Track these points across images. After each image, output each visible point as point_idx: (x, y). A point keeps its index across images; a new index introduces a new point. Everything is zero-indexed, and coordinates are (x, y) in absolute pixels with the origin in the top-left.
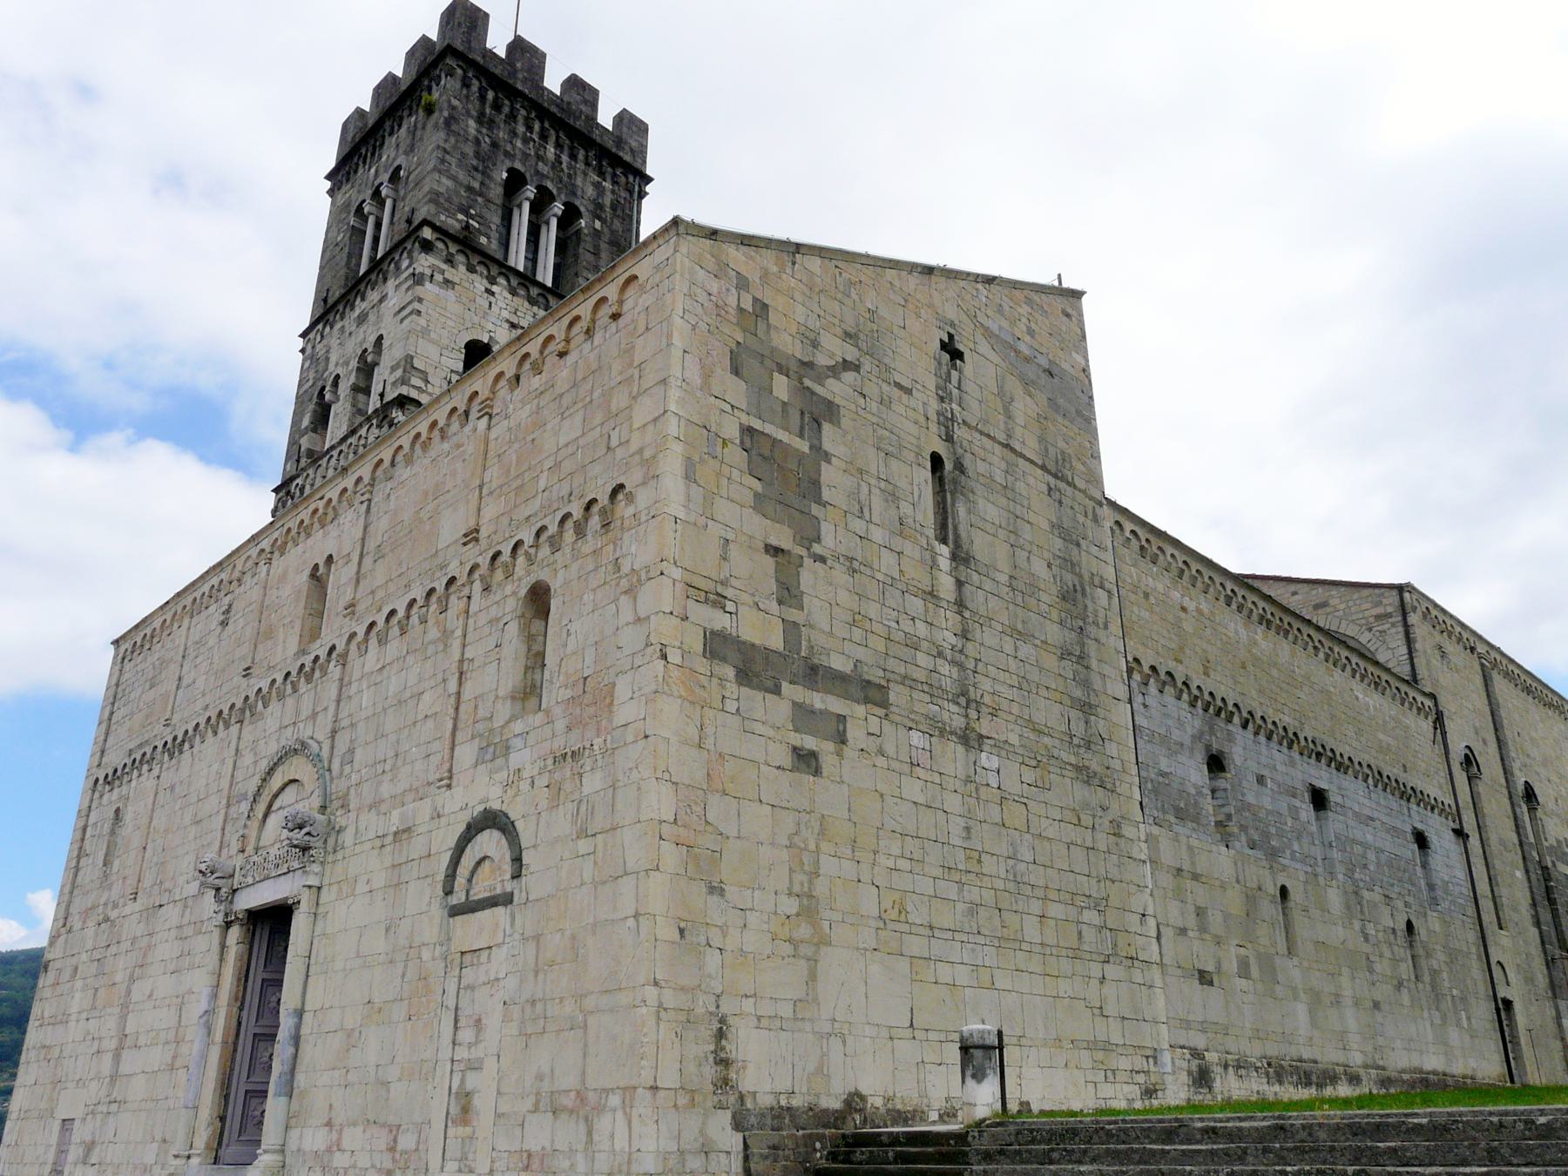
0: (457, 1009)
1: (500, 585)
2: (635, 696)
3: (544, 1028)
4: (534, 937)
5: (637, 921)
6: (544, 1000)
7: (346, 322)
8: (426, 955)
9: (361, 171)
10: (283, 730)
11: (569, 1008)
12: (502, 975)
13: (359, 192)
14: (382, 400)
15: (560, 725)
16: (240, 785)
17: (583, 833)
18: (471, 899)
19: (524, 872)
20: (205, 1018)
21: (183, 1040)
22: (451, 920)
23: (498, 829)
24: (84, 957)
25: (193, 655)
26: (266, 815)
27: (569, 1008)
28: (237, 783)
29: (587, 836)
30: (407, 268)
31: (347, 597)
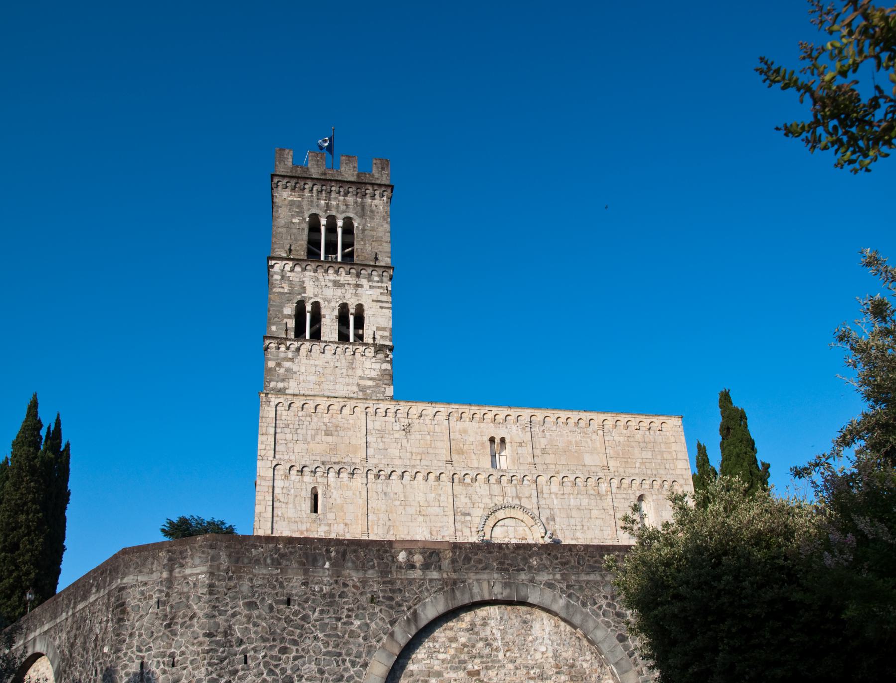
1: (625, 489)
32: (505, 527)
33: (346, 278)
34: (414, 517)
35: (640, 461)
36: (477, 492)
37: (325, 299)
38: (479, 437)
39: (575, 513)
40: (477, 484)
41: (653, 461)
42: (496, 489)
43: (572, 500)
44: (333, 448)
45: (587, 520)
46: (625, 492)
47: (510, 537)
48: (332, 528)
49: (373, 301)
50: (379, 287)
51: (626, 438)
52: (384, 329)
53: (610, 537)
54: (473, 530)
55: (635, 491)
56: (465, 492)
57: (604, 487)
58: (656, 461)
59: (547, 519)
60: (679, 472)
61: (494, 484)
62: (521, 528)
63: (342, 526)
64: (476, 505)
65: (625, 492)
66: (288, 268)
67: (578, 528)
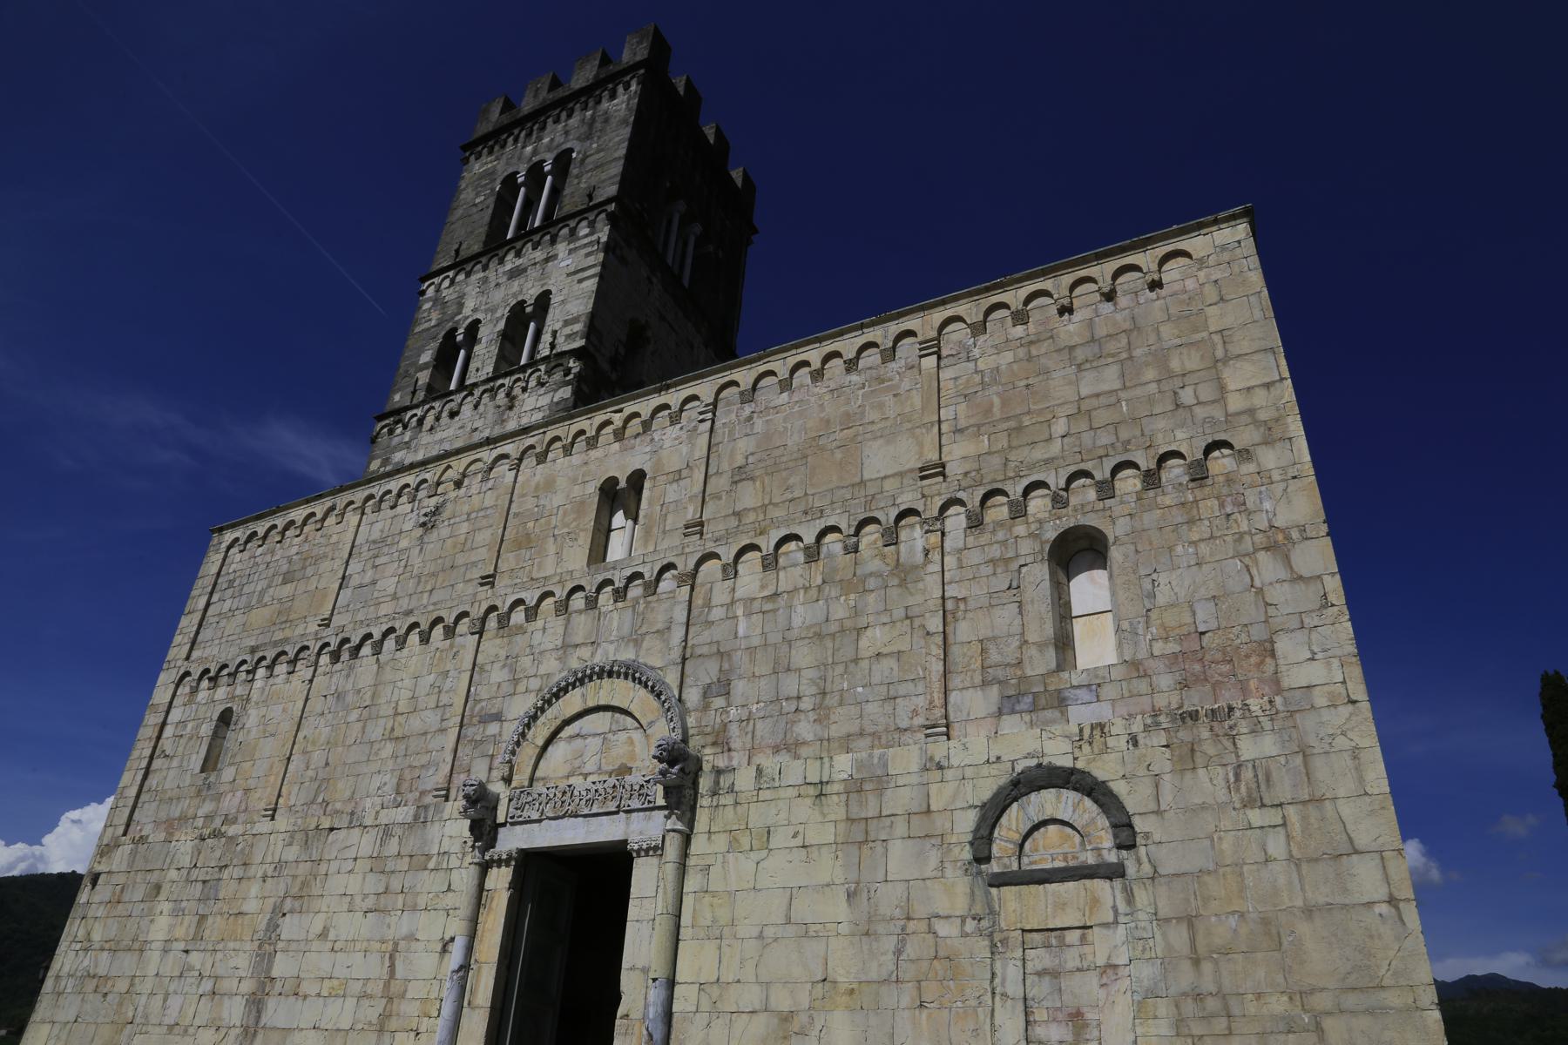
0: (1025, 999)
1: (999, 524)
2: (1316, 657)
3: (1229, 1028)
4: (1179, 919)
5: (1397, 908)
6: (1221, 995)
7: (491, 274)
8: (943, 928)
9: (510, 147)
10: (571, 650)
11: (1278, 1005)
12: (1123, 960)
13: (507, 164)
14: (551, 350)
15: (1165, 681)
16: (484, 704)
17: (1254, 801)
18: (1023, 868)
19: (1139, 840)
20: (461, 974)
21: (403, 996)
22: (994, 891)
23: (1075, 789)
24: (173, 874)
25: (366, 555)
26: (549, 741)
27: (1278, 1005)
28: (477, 702)
29: (1263, 806)
30: (586, 236)
31: (691, 513)
32: (579, 741)
33: (532, 256)
34: (376, 746)
35: (1072, 409)
36: (531, 646)
37: (486, 311)
38: (577, 491)
39: (803, 656)
40: (539, 623)
41: (1122, 395)
42: (582, 624)
43: (800, 609)
44: (284, 617)
45: (840, 669)
46: (1000, 535)
47: (589, 768)
48: (221, 805)
49: (568, 275)
50: (585, 246)
51: (1021, 352)
52: (575, 320)
53: (919, 721)
54: (496, 762)
55: (1040, 522)
56: (503, 654)
57: (914, 538)
58: (1138, 392)
59: (706, 693)
60: (1235, 403)
61: (580, 612)
62: (623, 736)
63: (239, 794)
64: (521, 688)
65: (1000, 535)
66: (446, 283)
67: (806, 704)
